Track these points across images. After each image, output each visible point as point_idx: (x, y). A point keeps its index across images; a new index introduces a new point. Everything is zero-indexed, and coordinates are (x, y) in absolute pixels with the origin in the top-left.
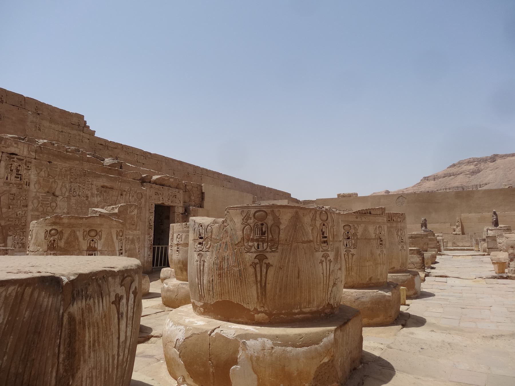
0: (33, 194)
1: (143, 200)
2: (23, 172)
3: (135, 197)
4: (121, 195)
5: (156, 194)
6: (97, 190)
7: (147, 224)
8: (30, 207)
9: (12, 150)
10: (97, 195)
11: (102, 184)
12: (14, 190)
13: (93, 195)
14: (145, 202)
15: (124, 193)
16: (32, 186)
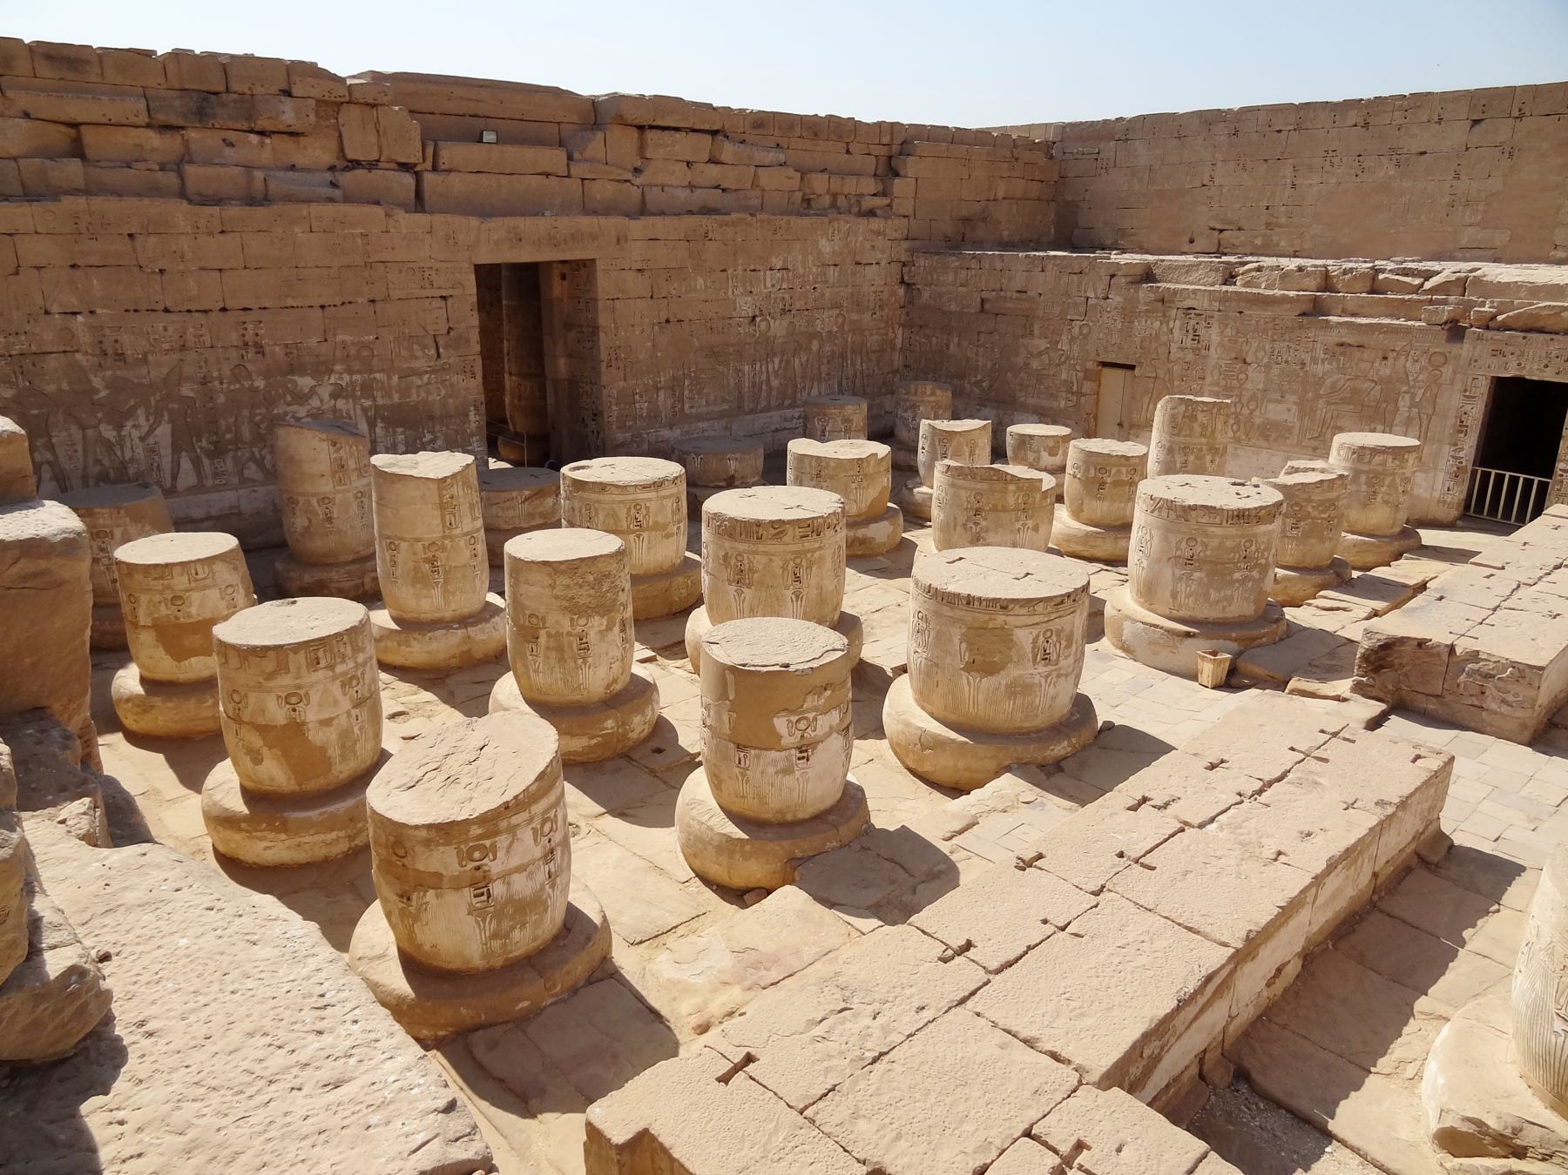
0: (1213, 362)
1: (1447, 371)
2: (1202, 332)
3: (1424, 362)
4: (1385, 358)
5: (1497, 353)
6: (1326, 351)
7: (1452, 421)
8: (1209, 379)
9: (1188, 303)
10: (1323, 360)
11: (1338, 340)
12: (1190, 357)
13: (1314, 361)
14: (1454, 372)
15: (1392, 355)
16: (1212, 350)
